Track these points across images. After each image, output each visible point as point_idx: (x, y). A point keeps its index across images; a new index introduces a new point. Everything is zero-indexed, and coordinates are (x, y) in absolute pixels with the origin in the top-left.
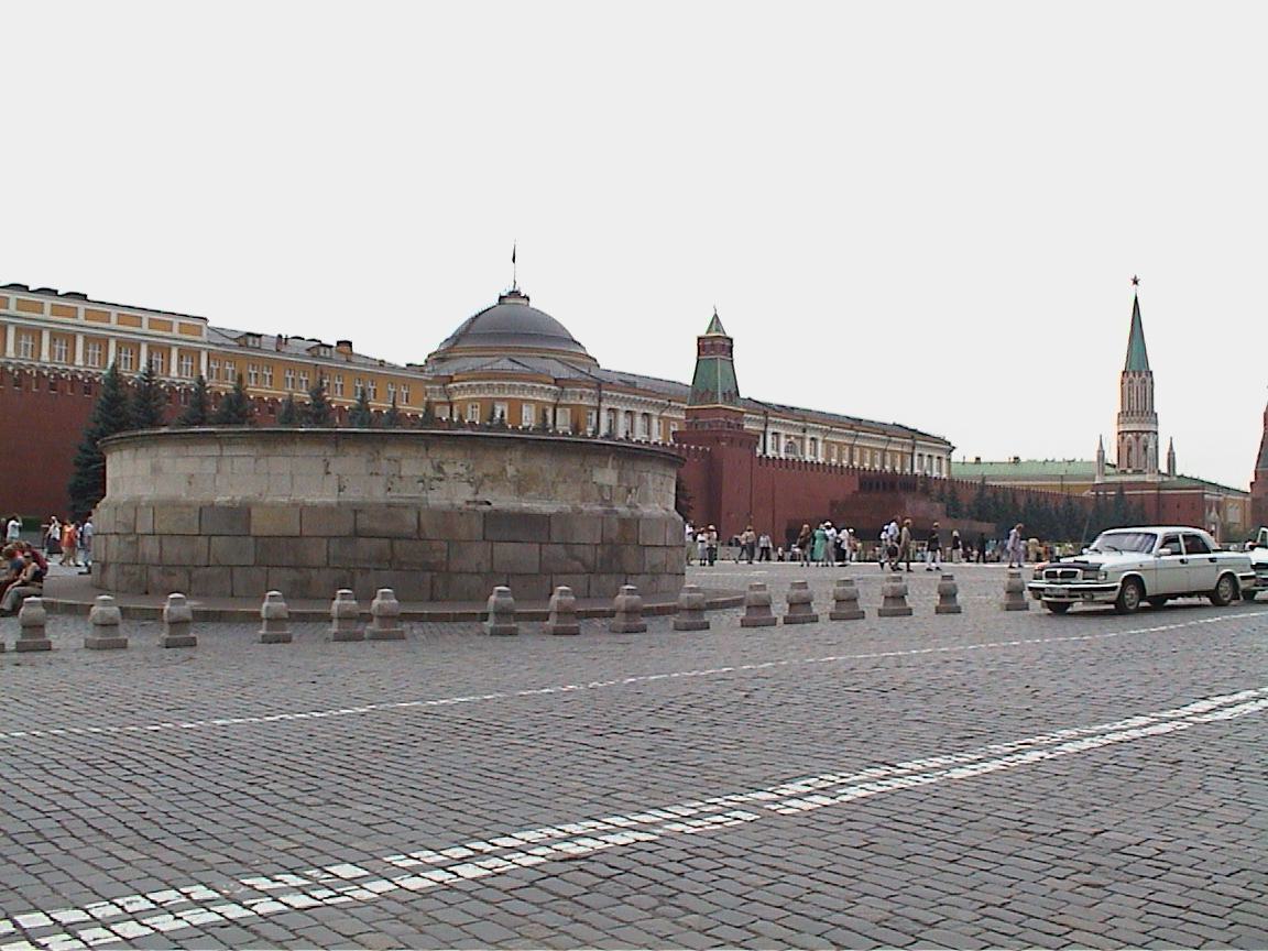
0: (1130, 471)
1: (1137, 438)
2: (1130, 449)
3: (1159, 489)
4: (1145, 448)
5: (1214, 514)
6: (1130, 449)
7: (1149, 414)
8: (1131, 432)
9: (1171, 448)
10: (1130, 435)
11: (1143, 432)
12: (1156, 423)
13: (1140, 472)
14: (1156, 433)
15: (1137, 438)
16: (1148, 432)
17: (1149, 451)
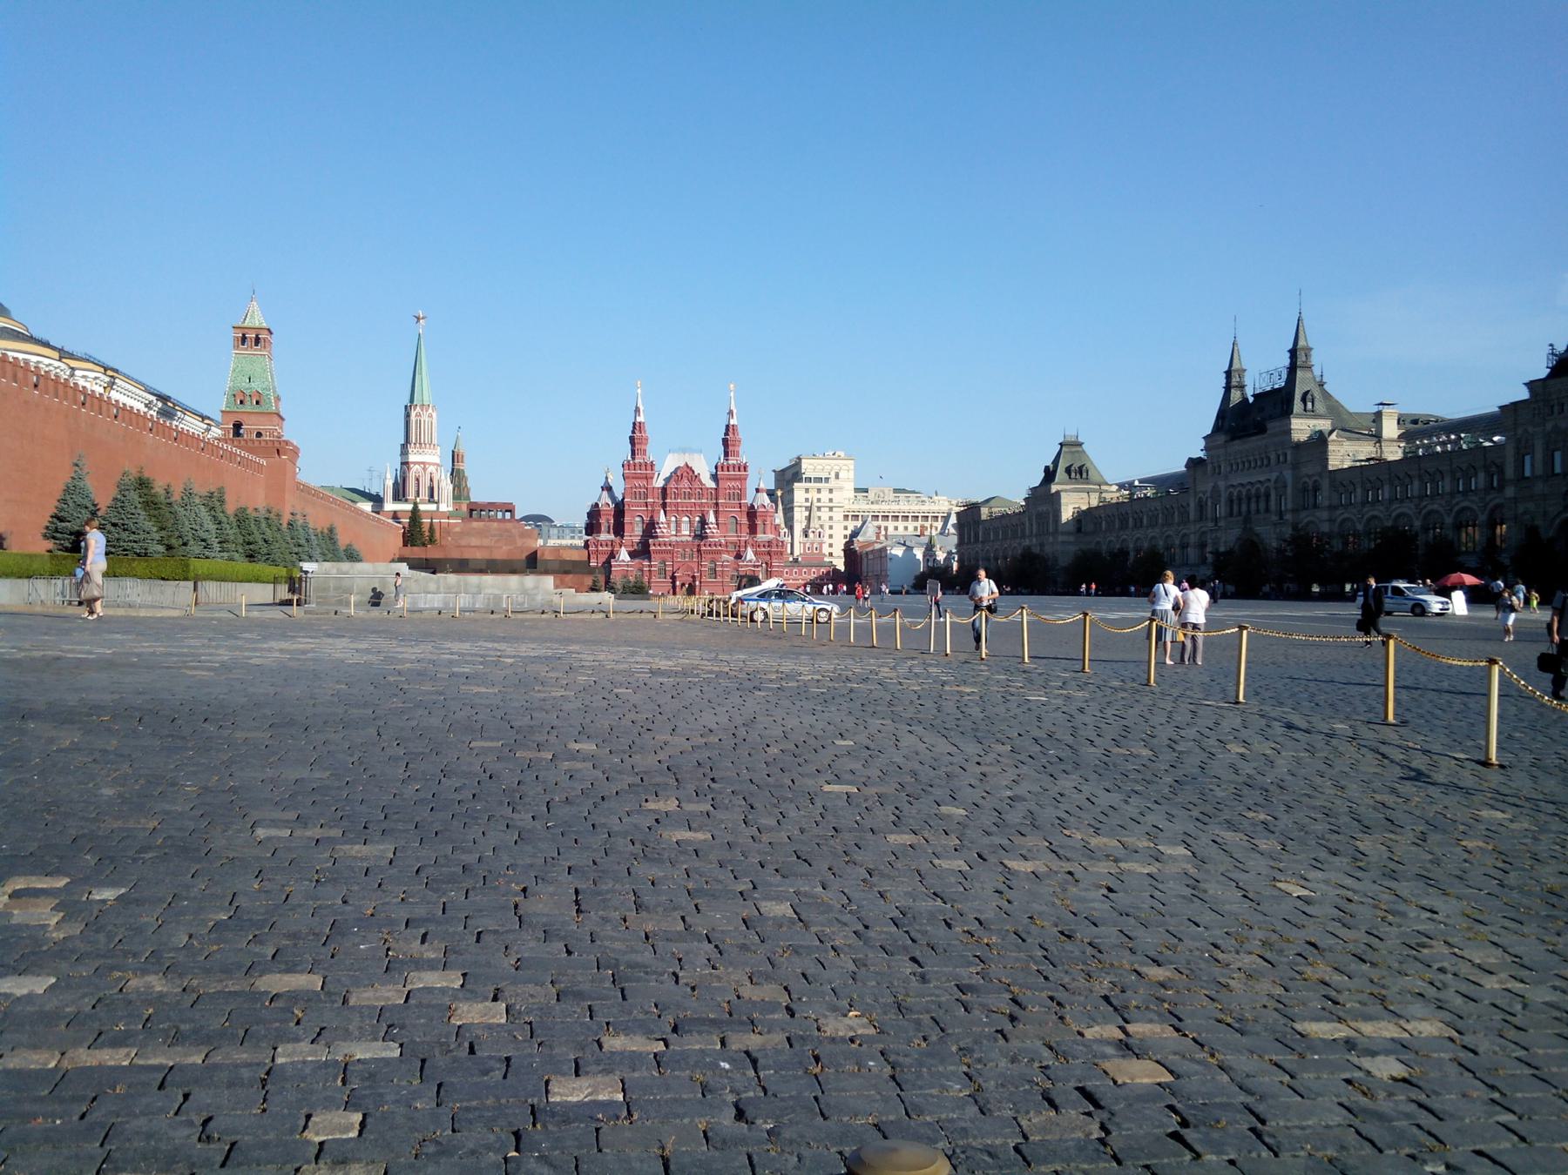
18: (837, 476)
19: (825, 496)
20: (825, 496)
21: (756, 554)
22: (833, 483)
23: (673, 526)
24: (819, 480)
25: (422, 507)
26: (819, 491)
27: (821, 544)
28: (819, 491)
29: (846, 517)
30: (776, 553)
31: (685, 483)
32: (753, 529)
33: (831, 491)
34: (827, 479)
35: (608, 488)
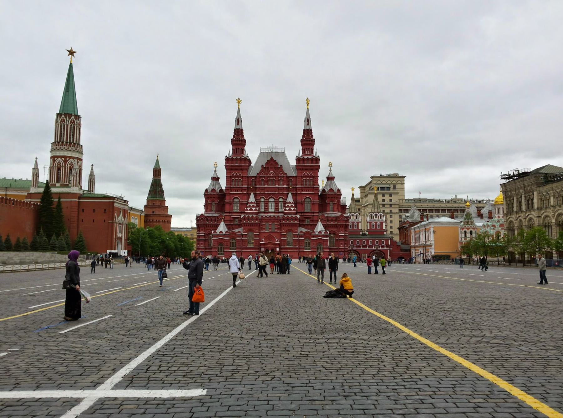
0: (58, 185)
1: (65, 162)
2: (59, 169)
3: (79, 198)
4: (71, 170)
5: (121, 217)
6: (59, 169)
7: (75, 144)
8: (61, 157)
9: (92, 169)
10: (59, 159)
11: (70, 157)
12: (81, 153)
13: (67, 186)
14: (81, 160)
15: (65, 162)
16: (74, 158)
17: (74, 171)
18: (394, 186)
19: (387, 198)
20: (387, 198)
21: (325, 226)
22: (391, 191)
23: (262, 205)
24: (383, 189)
25: (53, 190)
26: (383, 195)
27: (382, 223)
28: (383, 195)
29: (400, 211)
30: (341, 226)
31: (272, 173)
32: (323, 207)
33: (391, 195)
34: (389, 189)
35: (216, 179)
